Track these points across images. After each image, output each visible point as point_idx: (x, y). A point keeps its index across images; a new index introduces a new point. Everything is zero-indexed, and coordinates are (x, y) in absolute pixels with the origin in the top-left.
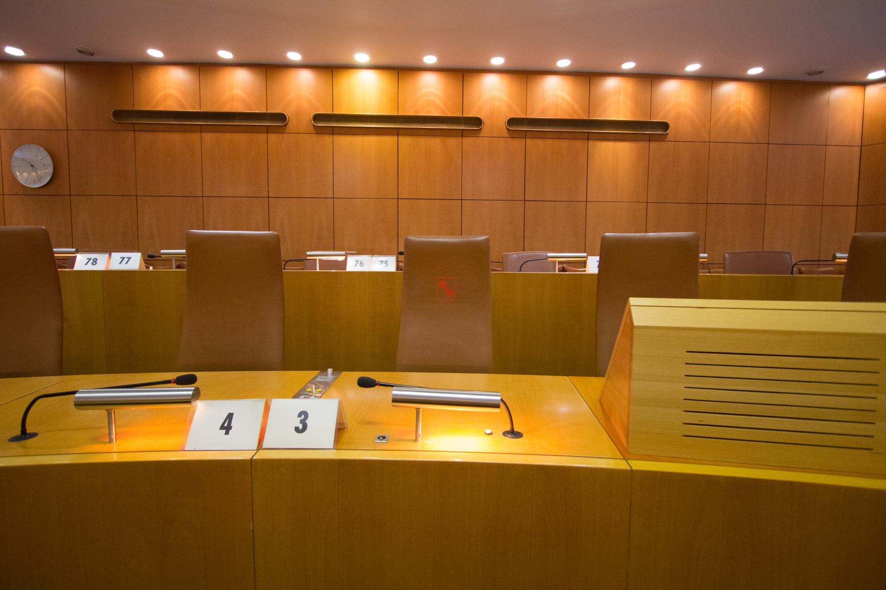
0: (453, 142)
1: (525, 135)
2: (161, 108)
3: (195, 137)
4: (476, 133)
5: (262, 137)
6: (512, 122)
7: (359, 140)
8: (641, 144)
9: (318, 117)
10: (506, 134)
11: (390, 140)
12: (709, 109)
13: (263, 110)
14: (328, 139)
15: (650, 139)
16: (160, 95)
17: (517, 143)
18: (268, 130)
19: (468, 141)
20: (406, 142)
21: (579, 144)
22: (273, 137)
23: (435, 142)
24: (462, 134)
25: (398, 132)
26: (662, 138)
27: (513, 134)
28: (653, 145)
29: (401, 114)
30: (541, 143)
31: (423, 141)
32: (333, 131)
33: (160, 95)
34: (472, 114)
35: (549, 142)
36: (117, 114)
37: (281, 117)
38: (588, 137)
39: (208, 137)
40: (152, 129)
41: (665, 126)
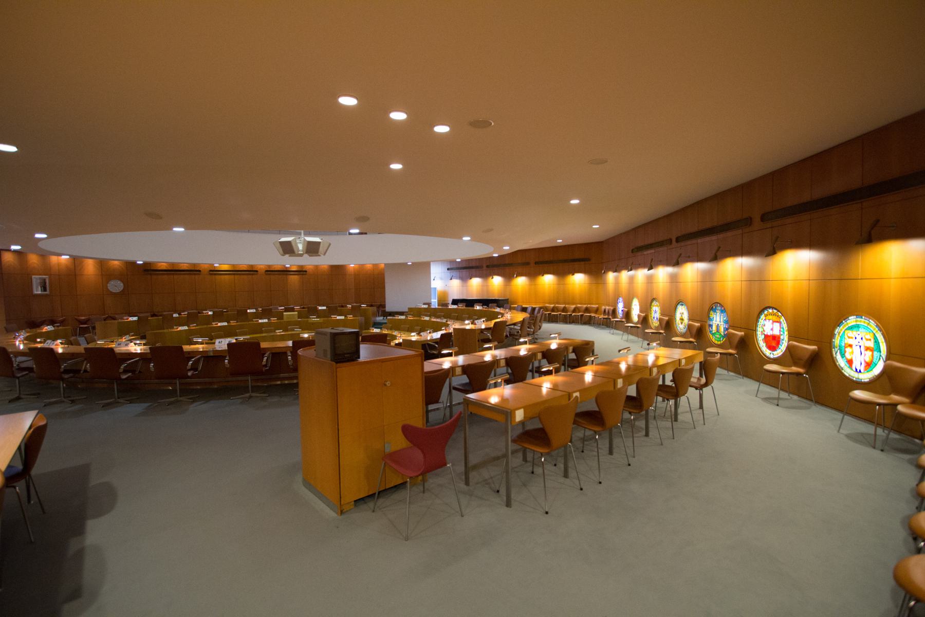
0: (250, 276)
1: (270, 274)
6: (266, 271)
7: (223, 277)
8: (300, 276)
9: (211, 271)
13: (193, 269)
15: (303, 274)
18: (195, 274)
20: (237, 277)
22: (197, 276)
24: (253, 274)
25: (234, 274)
26: (305, 274)
27: (266, 274)
28: (304, 276)
29: (235, 269)
31: (242, 276)
32: (215, 274)
34: (255, 269)
37: (200, 271)
38: (287, 274)
41: (306, 271)
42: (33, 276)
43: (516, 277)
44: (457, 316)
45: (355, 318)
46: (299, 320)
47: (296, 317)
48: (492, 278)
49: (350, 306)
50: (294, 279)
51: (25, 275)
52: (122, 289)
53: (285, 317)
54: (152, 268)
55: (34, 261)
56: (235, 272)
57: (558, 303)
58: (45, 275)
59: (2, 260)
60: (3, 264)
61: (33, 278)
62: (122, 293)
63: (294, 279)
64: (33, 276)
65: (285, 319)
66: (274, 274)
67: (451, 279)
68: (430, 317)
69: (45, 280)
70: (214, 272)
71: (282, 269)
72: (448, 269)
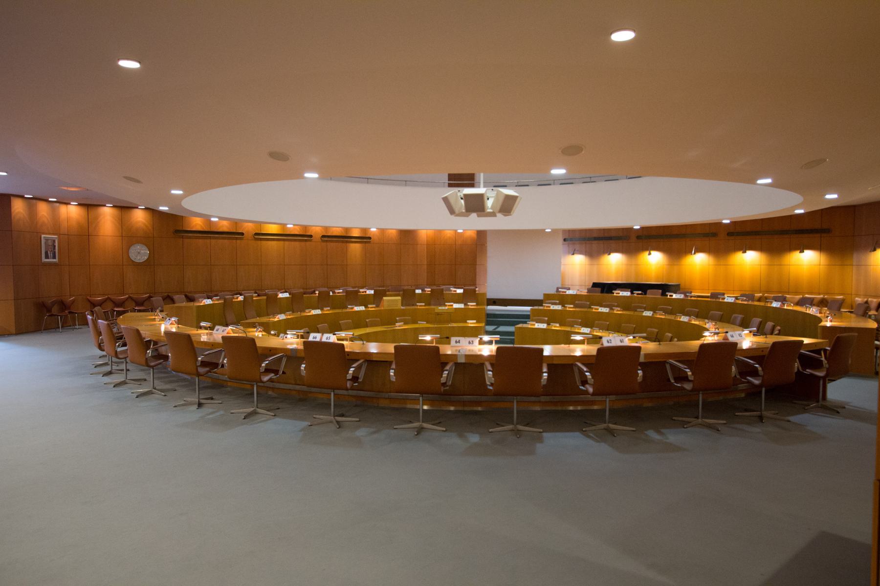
0: (303, 243)
1: (327, 241)
2: (194, 229)
3: (208, 241)
4: (311, 241)
5: (234, 241)
6: (323, 236)
9: (256, 234)
10: (320, 241)
11: (282, 243)
13: (234, 231)
14: (259, 242)
15: (366, 242)
16: (194, 223)
17: (324, 244)
18: (237, 239)
19: (308, 243)
20: (287, 243)
21: (344, 244)
22: (238, 241)
23: (297, 243)
24: (306, 241)
25: (284, 240)
27: (323, 241)
28: (367, 244)
29: (285, 233)
30: (332, 244)
31: (293, 243)
32: (261, 239)
33: (194, 223)
35: (334, 243)
36: (177, 232)
37: (242, 234)
38: (347, 242)
39: (213, 241)
40: (190, 238)
41: (370, 238)
42: (43, 236)
43: (695, 254)
44: (698, 312)
46: (402, 308)
47: (400, 303)
48: (650, 254)
49: (430, 290)
50: (355, 248)
51: (35, 230)
52: (146, 258)
54: (184, 229)
55: (45, 214)
56: (285, 236)
57: (768, 292)
58: (54, 234)
59: (12, 210)
60: (13, 215)
61: (42, 239)
62: (147, 264)
63: (355, 248)
64: (43, 236)
66: (332, 241)
67: (573, 254)
68: (654, 312)
69: (54, 241)
70: (259, 236)
71: (343, 235)
72: (565, 240)
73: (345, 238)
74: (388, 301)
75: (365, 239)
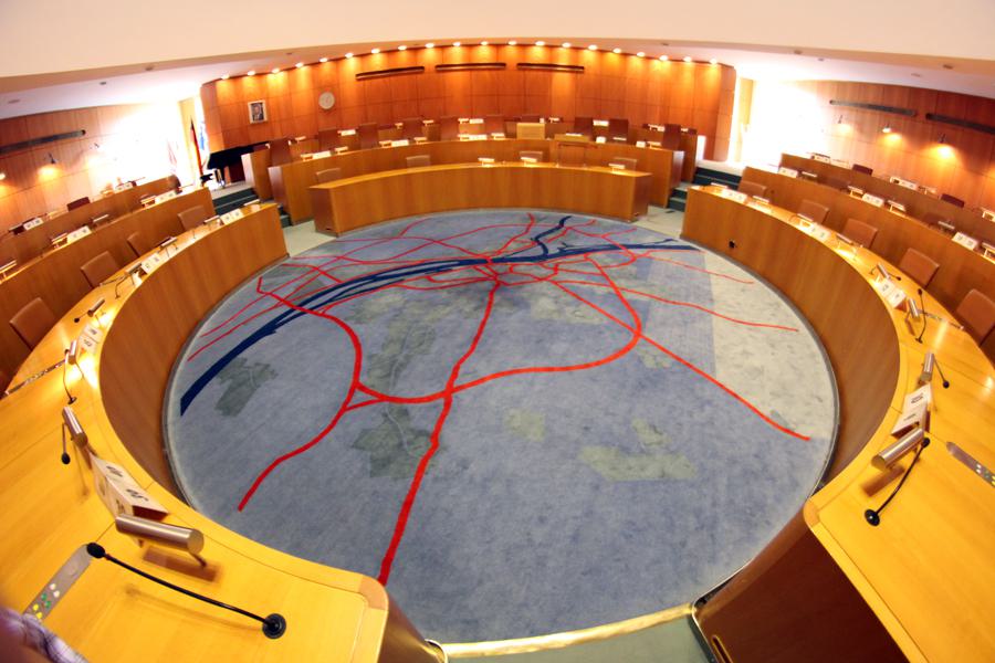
0: (494, 73)
1: (525, 70)
5: (414, 76)
6: (519, 64)
9: (438, 66)
12: (601, 63)
14: (441, 74)
17: (521, 73)
22: (419, 76)
27: (519, 69)
32: (444, 71)
37: (422, 68)
38: (551, 71)
41: (582, 68)
45: (665, 150)
53: (519, 132)
65: (520, 137)
73: (550, 67)
74: (525, 128)
75: (575, 69)
